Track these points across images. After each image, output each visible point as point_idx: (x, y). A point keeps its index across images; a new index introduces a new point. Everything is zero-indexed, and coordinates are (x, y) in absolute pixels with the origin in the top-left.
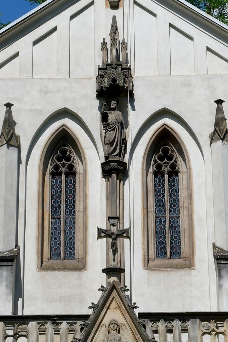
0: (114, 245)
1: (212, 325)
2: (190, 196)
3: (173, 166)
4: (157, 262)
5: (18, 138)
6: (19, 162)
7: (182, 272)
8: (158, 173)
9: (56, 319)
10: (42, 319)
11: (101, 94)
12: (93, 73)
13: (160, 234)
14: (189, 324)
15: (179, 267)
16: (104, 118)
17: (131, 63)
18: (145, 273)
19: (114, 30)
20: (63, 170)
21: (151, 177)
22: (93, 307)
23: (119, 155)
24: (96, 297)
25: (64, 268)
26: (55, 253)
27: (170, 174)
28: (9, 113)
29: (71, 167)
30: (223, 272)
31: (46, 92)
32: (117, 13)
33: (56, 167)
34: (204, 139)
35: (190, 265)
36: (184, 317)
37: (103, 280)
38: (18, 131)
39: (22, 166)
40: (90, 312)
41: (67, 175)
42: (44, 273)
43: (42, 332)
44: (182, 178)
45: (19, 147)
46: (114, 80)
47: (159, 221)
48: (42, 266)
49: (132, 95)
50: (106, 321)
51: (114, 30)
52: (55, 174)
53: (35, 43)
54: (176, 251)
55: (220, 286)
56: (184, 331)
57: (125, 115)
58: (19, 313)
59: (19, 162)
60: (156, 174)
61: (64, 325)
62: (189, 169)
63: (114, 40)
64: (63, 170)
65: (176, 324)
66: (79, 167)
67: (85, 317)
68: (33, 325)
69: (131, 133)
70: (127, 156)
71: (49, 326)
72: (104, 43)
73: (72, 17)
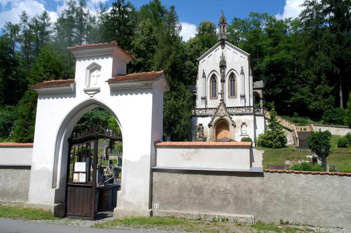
0: (221, 96)
1: (238, 109)
2: (237, 85)
3: (234, 79)
4: (231, 97)
5: (205, 76)
6: (206, 80)
7: (235, 99)
8: (231, 81)
9: (212, 109)
10: (210, 109)
11: (220, 67)
12: (219, 63)
13: (231, 92)
14: (234, 109)
15: (234, 98)
16: (221, 71)
17: (226, 61)
18: (228, 99)
19: (223, 54)
20: (214, 81)
21: (230, 81)
22: (218, 106)
23: (224, 78)
24: (219, 105)
25: (214, 99)
26: (213, 96)
27: (233, 81)
28: (204, 72)
29: (215, 80)
30: (242, 99)
31: (211, 67)
32: (223, 50)
33: (213, 81)
34: (239, 74)
35: (236, 98)
36: (234, 108)
37: (220, 102)
38: (205, 75)
39: (207, 81)
41: (215, 82)
42: (212, 100)
43: (209, 110)
44: (235, 81)
45: (206, 78)
46: (222, 64)
47: (231, 90)
48: (210, 98)
49: (226, 67)
50: (220, 109)
51: (223, 54)
52: (213, 82)
54: (234, 95)
55: (241, 102)
56: (234, 109)
57: (225, 70)
58: (207, 108)
59: (206, 80)
60: (231, 81)
61: (213, 109)
62: (237, 80)
63: (222, 56)
64: (214, 81)
65: (232, 109)
66: (217, 80)
67: (217, 108)
68: (208, 109)
69: (226, 73)
70: (225, 78)
71: (211, 110)
72: (221, 57)
73: (215, 52)
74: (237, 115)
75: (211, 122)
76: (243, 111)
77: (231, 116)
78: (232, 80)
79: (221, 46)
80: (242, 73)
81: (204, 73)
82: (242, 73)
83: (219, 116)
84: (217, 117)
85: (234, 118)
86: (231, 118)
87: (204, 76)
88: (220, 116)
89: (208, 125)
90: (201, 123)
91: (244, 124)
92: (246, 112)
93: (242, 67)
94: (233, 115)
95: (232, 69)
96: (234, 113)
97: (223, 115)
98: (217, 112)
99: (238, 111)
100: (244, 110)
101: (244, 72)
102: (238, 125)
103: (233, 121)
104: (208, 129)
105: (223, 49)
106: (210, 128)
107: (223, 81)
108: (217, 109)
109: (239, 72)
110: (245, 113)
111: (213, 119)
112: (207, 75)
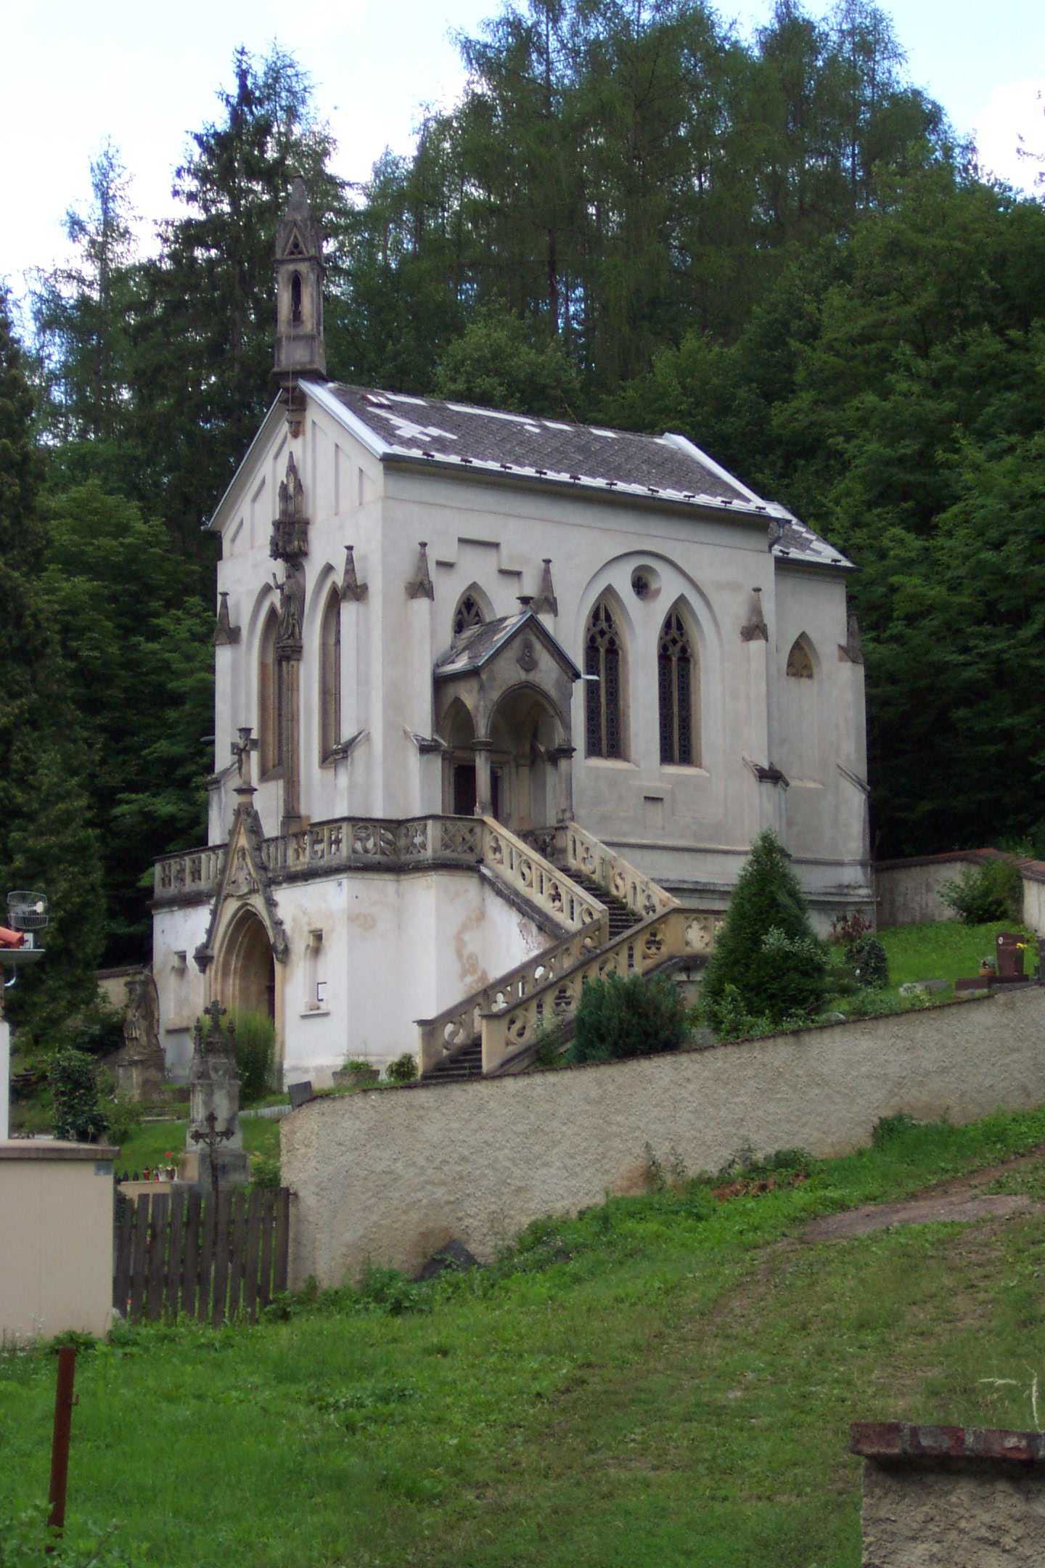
32: (295, 446)
53: (255, 499)
71: (213, 857)
75: (210, 932)
111: (215, 914)
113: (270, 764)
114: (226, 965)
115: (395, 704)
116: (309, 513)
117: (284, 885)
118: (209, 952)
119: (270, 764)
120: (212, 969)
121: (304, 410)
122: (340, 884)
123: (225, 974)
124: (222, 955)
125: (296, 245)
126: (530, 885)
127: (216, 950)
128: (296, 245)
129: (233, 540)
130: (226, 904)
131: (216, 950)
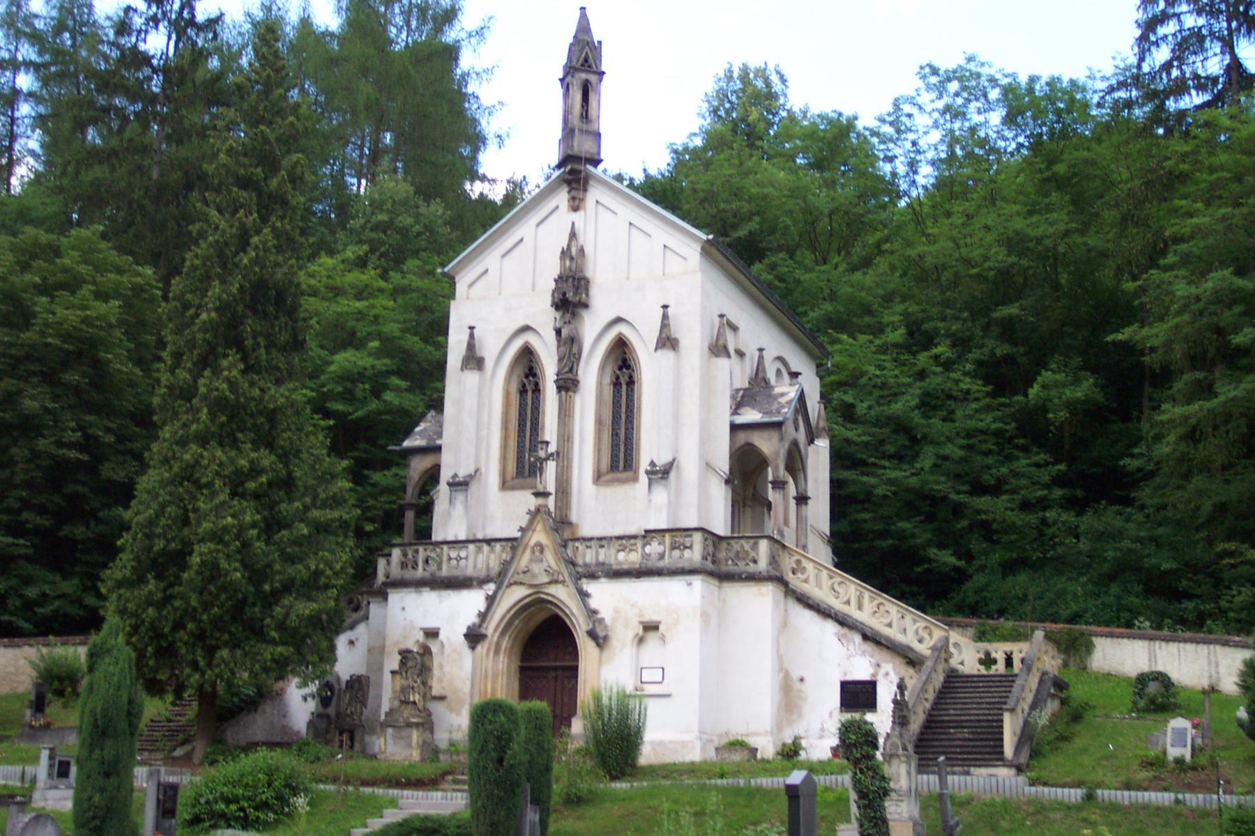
4: (610, 476)
8: (616, 384)
22: (521, 529)
24: (524, 521)
28: (472, 336)
32: (577, 217)
38: (479, 353)
40: (518, 534)
47: (615, 435)
51: (573, 235)
53: (504, 256)
61: (498, 546)
67: (515, 539)
68: (471, 547)
71: (486, 548)
74: (618, 574)
75: (483, 616)
76: (646, 556)
77: (588, 586)
78: (623, 380)
79: (569, 192)
80: (667, 341)
81: (471, 346)
82: (667, 341)
83: (521, 583)
84: (514, 588)
85: (604, 595)
86: (584, 595)
87: (473, 360)
88: (531, 586)
89: (466, 636)
90: (431, 624)
91: (651, 627)
92: (666, 563)
93: (665, 307)
94: (592, 576)
95: (619, 320)
96: (603, 564)
97: (546, 579)
98: (512, 558)
99: (621, 556)
100: (654, 548)
101: (677, 330)
102: (623, 636)
103: (595, 612)
104: (467, 655)
105: (575, 209)
106: (473, 648)
107: (568, 384)
108: (513, 544)
109: (652, 334)
110: (661, 564)
111: (491, 600)
112: (489, 350)
113: (508, 477)
114: (498, 645)
115: (705, 440)
116: (589, 273)
117: (603, 580)
118: (483, 631)
119: (508, 477)
120: (482, 648)
121: (585, 190)
122: (689, 584)
123: (497, 652)
124: (497, 634)
125: (586, 60)
126: (848, 602)
127: (491, 629)
128: (586, 60)
129: (470, 286)
130: (508, 591)
131: (491, 629)
